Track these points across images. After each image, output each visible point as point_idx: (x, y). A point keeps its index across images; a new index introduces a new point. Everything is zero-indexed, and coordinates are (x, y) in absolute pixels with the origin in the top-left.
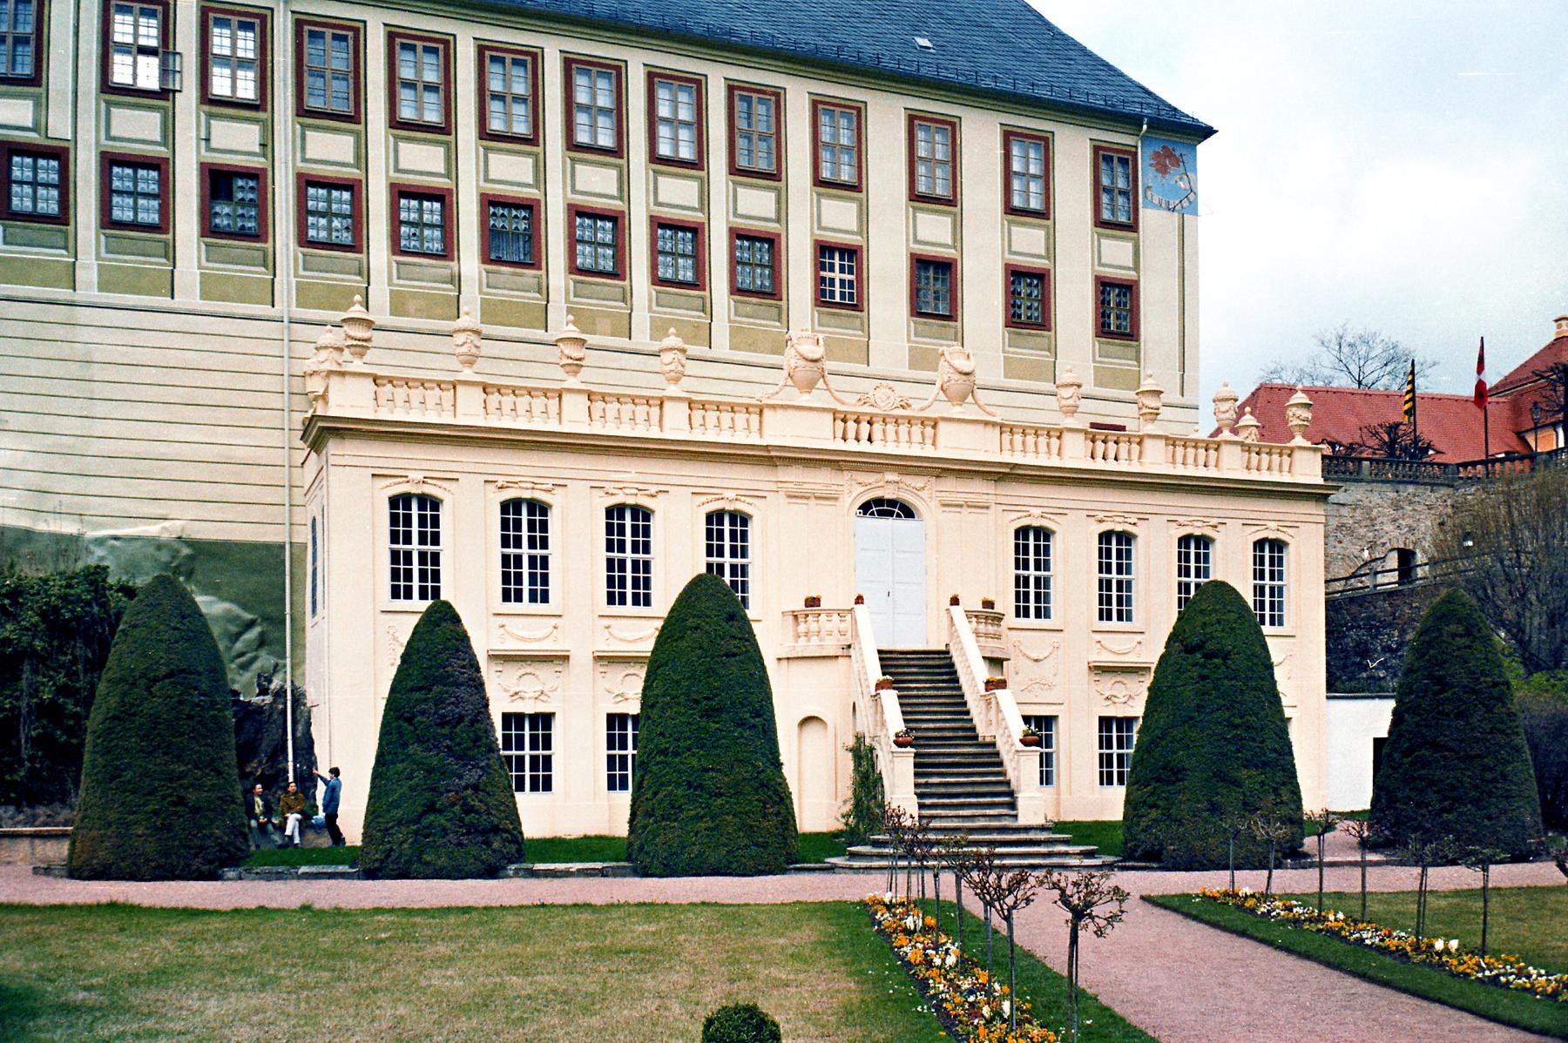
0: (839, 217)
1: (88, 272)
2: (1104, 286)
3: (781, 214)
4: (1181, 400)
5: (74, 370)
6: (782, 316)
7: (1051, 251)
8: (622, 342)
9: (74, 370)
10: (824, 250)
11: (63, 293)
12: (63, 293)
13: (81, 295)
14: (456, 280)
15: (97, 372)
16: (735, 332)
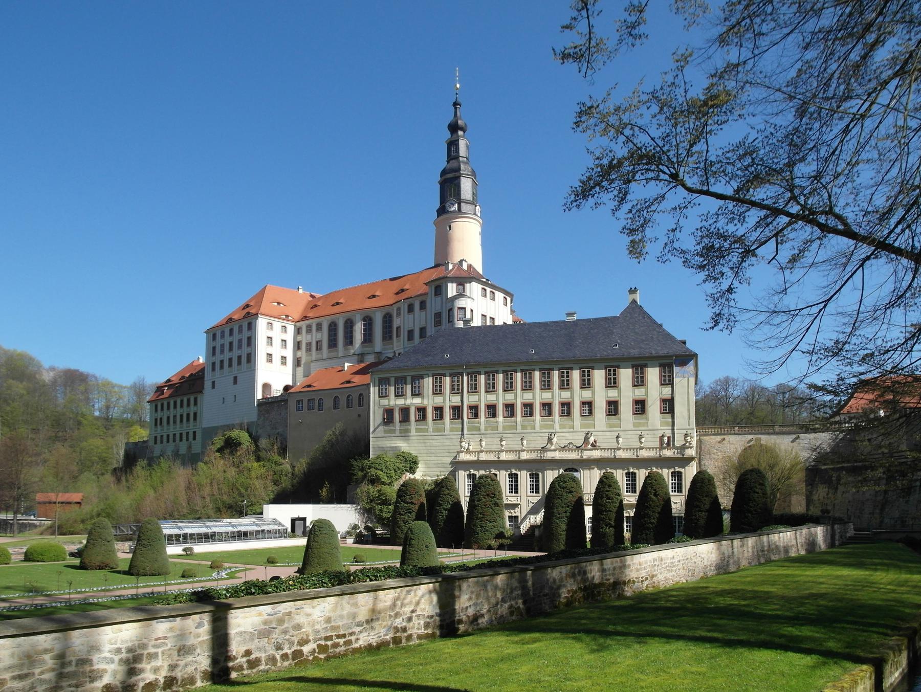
0: (587, 395)
1: (431, 429)
2: (664, 401)
3: (572, 397)
4: (688, 427)
5: (429, 448)
6: (573, 420)
7: (647, 394)
8: (534, 431)
9: (429, 448)
10: (584, 403)
11: (426, 434)
12: (426, 434)
13: (429, 434)
14: (497, 422)
15: (432, 448)
16: (560, 425)
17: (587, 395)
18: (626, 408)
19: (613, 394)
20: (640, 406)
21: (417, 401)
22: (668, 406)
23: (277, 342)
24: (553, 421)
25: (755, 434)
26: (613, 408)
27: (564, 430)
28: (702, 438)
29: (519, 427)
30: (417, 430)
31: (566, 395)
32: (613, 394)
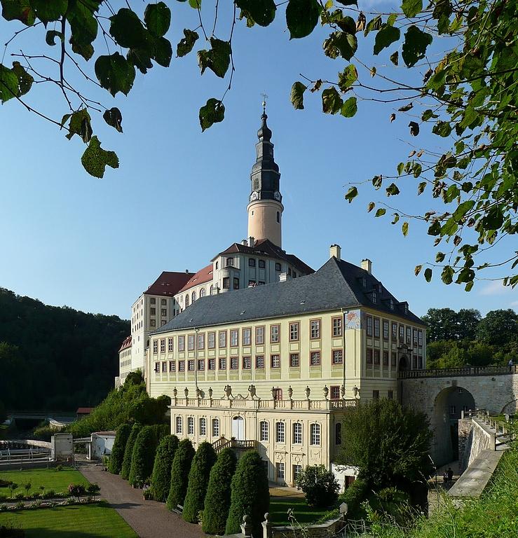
0: (275, 349)
4: (355, 377)
6: (264, 372)
17: (275, 349)
18: (305, 360)
19: (295, 347)
20: (315, 358)
21: (171, 356)
22: (338, 357)
23: (158, 312)
24: (251, 372)
25: (451, 376)
26: (294, 359)
27: (260, 381)
28: (404, 380)
29: (228, 377)
30: (171, 379)
31: (260, 350)
32: (295, 347)
